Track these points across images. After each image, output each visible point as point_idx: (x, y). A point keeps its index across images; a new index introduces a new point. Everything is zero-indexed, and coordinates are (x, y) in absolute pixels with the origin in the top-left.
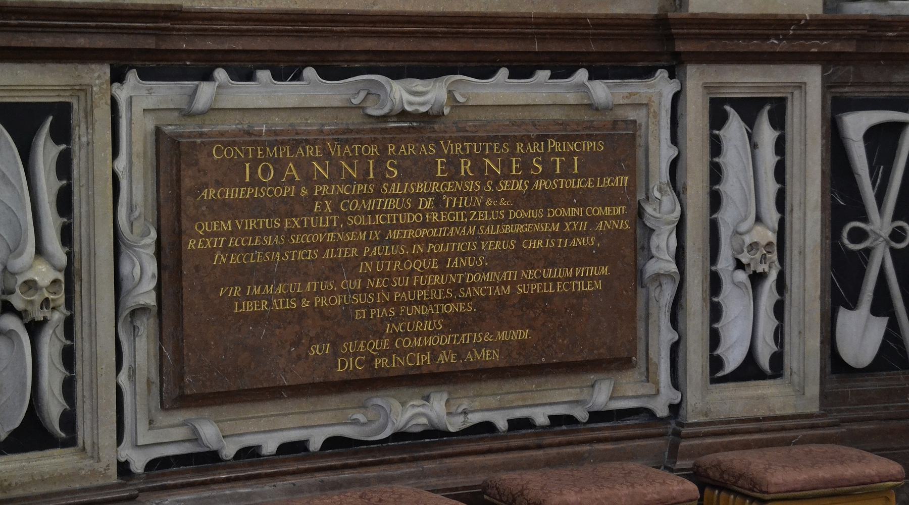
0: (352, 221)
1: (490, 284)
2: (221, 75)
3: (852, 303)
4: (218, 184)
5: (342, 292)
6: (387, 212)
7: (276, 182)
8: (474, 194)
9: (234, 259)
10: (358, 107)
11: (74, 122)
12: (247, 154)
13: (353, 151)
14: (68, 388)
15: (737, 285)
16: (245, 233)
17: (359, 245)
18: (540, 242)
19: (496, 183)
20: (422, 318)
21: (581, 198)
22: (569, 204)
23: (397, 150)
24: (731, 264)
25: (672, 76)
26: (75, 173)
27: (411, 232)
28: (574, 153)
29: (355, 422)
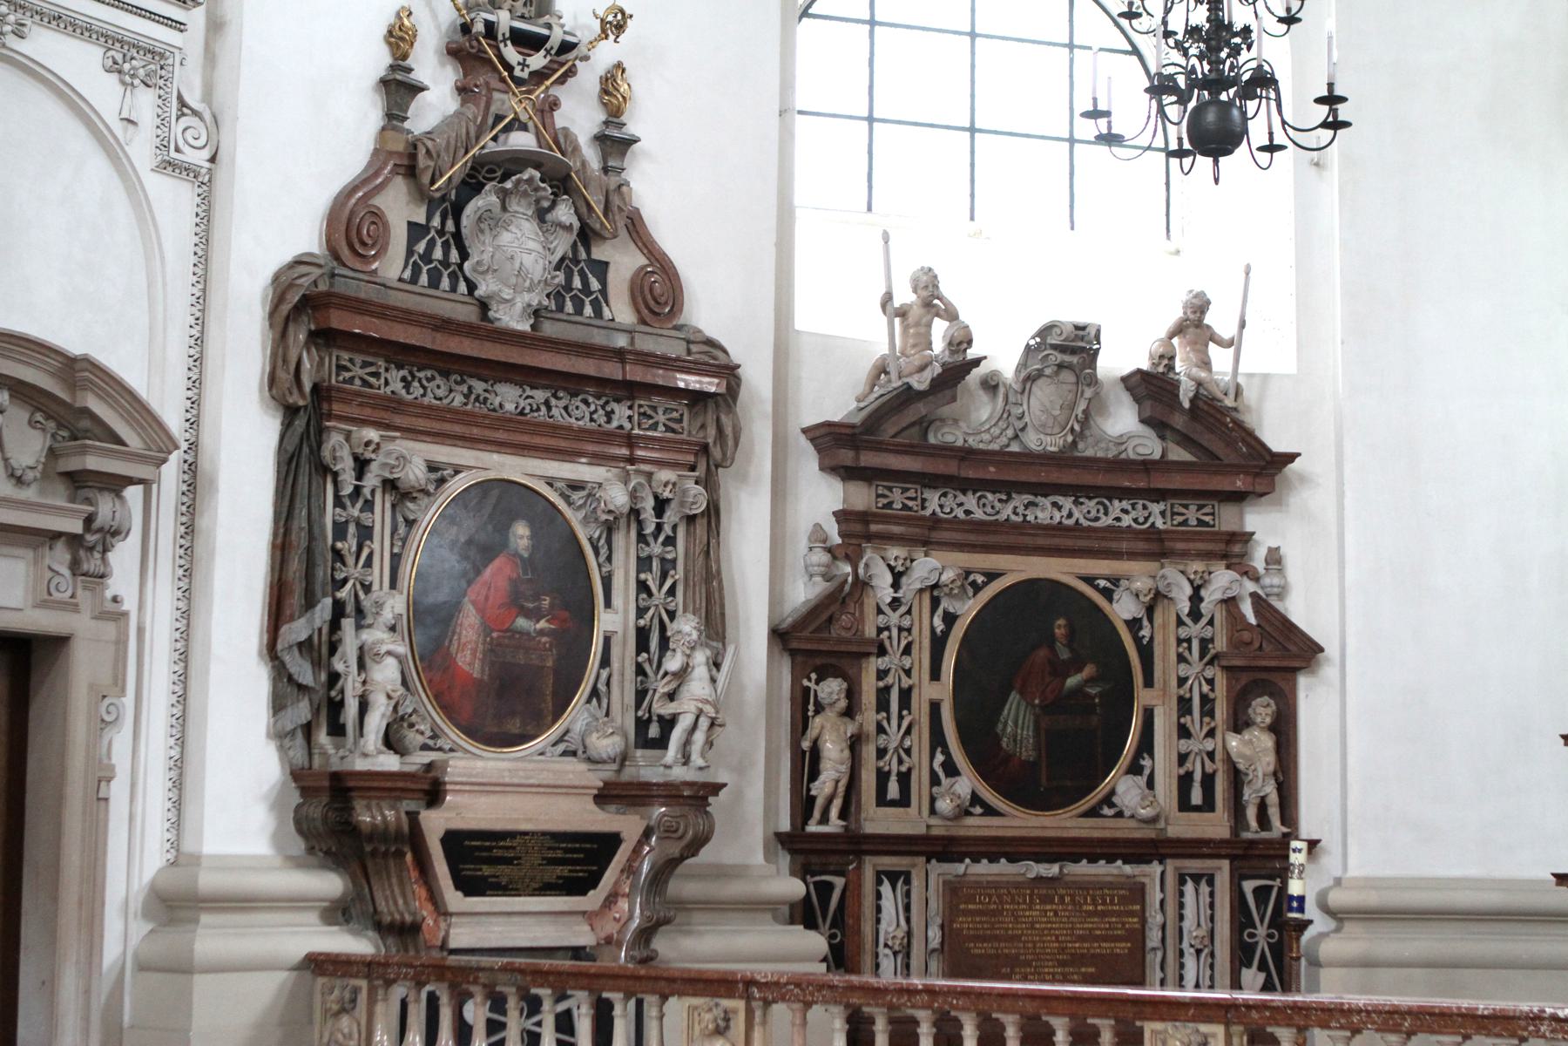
3: (1249, 966)
4: (965, 903)
7: (989, 903)
9: (972, 932)
15: (1191, 954)
16: (976, 922)
21: (1119, 914)
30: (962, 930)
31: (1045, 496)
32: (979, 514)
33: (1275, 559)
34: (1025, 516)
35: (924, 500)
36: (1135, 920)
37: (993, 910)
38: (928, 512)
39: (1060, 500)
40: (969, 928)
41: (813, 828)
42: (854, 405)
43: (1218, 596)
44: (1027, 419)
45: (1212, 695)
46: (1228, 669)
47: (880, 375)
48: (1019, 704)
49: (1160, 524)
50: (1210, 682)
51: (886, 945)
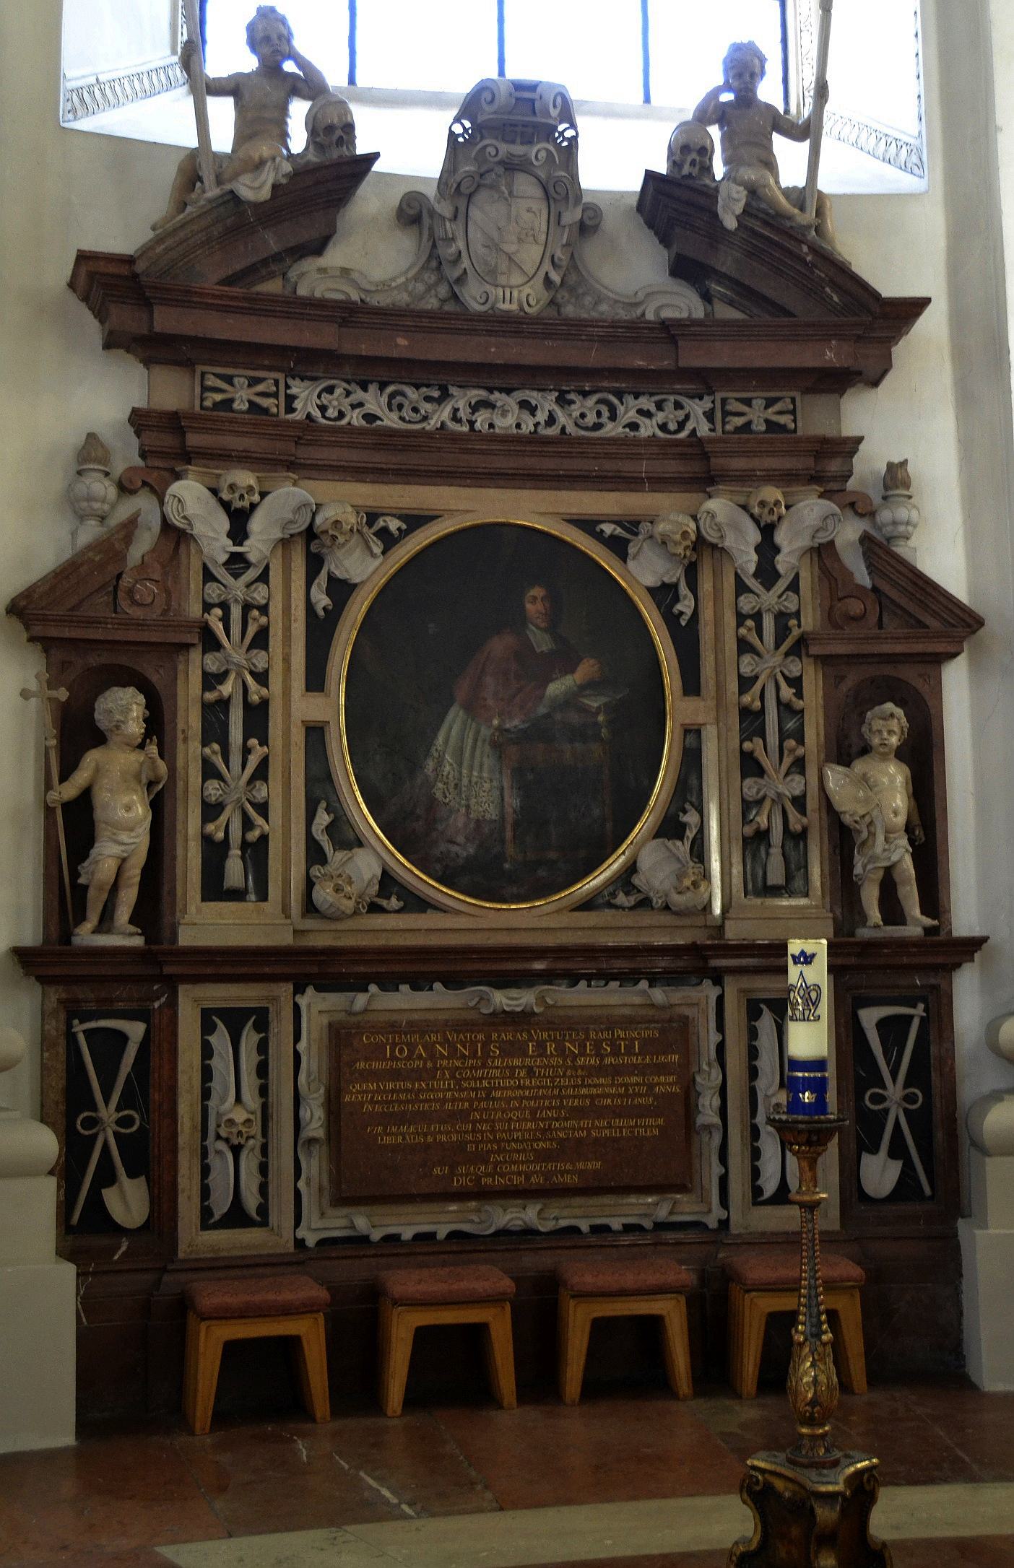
0: (465, 1085)
1: (570, 1129)
2: (373, 988)
3: (874, 1150)
4: (366, 1059)
5: (458, 1132)
6: (491, 1078)
7: (409, 1058)
8: (558, 1066)
9: (378, 1108)
10: (473, 1008)
11: (270, 1019)
12: (387, 1040)
13: (466, 1037)
14: (263, 1189)
15: (769, 1133)
16: (385, 1091)
17: (471, 1101)
18: (609, 1101)
19: (575, 1057)
20: (518, 1151)
21: (642, 1070)
22: (631, 1074)
23: (499, 1037)
24: (765, 1120)
25: (715, 984)
26: (270, 1051)
27: (509, 1093)
28: (636, 1039)
29: (472, 1221)
30: (362, 1104)
31: (508, 391)
32: (391, 420)
33: (896, 477)
34: (472, 423)
35: (290, 399)
36: (672, 1079)
37: (417, 1070)
38: (298, 416)
39: (533, 397)
40: (372, 1101)
41: (86, 935)
42: (151, 235)
43: (804, 542)
44: (465, 263)
45: (799, 704)
46: (825, 661)
47: (194, 186)
48: (463, 729)
49: (704, 429)
50: (796, 683)
51: (218, 1137)
